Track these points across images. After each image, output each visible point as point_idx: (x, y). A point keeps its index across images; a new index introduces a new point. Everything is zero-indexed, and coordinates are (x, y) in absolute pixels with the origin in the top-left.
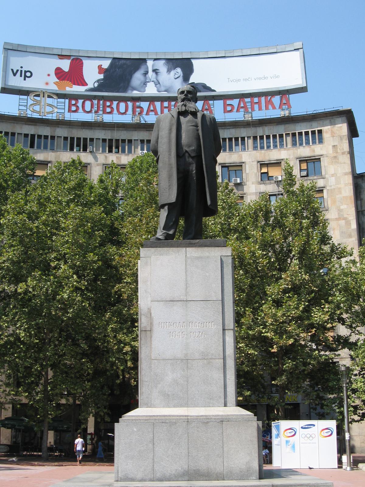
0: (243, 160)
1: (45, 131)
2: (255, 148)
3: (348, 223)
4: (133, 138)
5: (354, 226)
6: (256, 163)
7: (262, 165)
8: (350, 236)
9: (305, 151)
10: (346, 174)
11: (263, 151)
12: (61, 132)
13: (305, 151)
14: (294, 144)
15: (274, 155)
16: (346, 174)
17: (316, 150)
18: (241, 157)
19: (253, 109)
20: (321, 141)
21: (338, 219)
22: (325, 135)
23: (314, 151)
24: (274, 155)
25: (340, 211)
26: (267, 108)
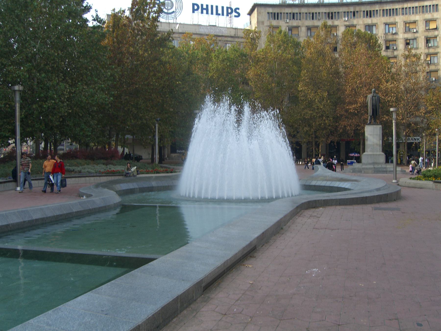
0: (397, 21)
1: (296, 10)
2: (403, 14)
4: (340, 11)
6: (403, 22)
7: (406, 23)
9: (428, 16)
11: (407, 16)
13: (428, 16)
14: (423, 12)
15: (413, 18)
20: (437, 10)
23: (433, 16)
24: (413, 18)
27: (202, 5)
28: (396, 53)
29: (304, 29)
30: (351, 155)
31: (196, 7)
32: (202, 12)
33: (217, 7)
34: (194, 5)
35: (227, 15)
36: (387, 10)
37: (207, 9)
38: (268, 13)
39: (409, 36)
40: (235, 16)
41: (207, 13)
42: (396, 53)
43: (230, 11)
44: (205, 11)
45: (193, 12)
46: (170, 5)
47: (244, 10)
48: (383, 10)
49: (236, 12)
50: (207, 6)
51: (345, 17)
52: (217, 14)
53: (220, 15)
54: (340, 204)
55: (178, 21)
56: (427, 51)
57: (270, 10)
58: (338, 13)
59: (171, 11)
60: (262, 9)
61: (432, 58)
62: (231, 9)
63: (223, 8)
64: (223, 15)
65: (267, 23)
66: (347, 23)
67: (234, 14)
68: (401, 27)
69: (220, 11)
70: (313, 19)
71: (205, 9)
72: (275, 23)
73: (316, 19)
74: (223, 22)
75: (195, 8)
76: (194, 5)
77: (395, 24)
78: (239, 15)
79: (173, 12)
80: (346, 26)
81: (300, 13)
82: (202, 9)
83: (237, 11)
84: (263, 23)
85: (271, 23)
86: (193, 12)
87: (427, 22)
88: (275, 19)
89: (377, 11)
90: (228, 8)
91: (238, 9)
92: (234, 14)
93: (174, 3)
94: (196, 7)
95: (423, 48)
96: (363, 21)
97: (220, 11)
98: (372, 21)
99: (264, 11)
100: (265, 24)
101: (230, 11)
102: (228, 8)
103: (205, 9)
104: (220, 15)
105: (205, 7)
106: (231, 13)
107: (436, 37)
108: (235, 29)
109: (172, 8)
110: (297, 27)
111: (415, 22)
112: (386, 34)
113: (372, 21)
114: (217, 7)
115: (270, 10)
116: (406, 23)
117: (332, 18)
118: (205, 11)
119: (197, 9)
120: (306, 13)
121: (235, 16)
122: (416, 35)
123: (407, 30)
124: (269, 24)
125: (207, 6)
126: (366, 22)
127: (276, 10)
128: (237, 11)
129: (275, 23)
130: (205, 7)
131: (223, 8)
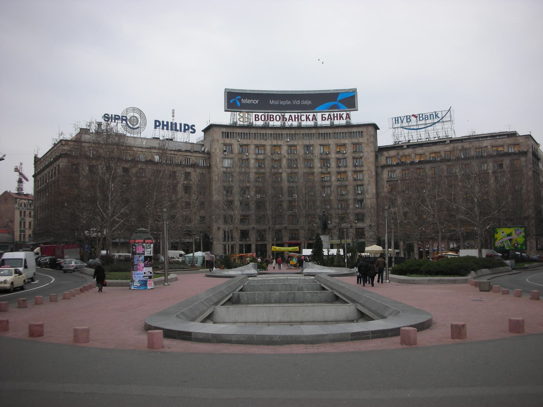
3: (371, 172)
5: (374, 174)
7: (337, 145)
8: (372, 178)
10: (372, 151)
12: (253, 131)
13: (355, 141)
16: (372, 151)
17: (361, 140)
19: (334, 119)
20: (362, 136)
21: (367, 170)
22: (364, 134)
24: (343, 141)
25: (368, 167)
26: (340, 119)
27: (163, 122)
28: (329, 170)
29: (252, 147)
31: (158, 124)
32: (163, 129)
34: (156, 121)
35: (185, 131)
37: (167, 125)
38: (223, 132)
39: (340, 156)
40: (191, 132)
42: (329, 170)
43: (187, 127)
44: (165, 127)
45: (155, 128)
47: (200, 127)
48: (319, 134)
53: (178, 131)
54: (373, 338)
55: (143, 136)
56: (354, 169)
57: (224, 130)
58: (282, 134)
59: (136, 127)
61: (358, 175)
63: (181, 124)
64: (181, 131)
66: (289, 143)
69: (178, 128)
72: (228, 141)
73: (263, 139)
74: (180, 137)
75: (157, 124)
76: (156, 121)
78: (194, 131)
79: (138, 127)
81: (250, 133)
82: (163, 125)
85: (225, 141)
86: (155, 128)
87: (355, 144)
88: (228, 137)
91: (194, 126)
92: (190, 130)
93: (139, 120)
94: (158, 124)
95: (351, 166)
97: (178, 128)
100: (220, 142)
101: (187, 127)
102: (185, 125)
104: (178, 131)
106: (188, 129)
107: (361, 158)
108: (192, 143)
109: (137, 124)
110: (247, 145)
116: (337, 145)
117: (276, 139)
118: (165, 127)
120: (255, 134)
121: (191, 132)
122: (345, 156)
125: (167, 122)
126: (304, 143)
127: (229, 130)
129: (228, 141)
131: (181, 124)
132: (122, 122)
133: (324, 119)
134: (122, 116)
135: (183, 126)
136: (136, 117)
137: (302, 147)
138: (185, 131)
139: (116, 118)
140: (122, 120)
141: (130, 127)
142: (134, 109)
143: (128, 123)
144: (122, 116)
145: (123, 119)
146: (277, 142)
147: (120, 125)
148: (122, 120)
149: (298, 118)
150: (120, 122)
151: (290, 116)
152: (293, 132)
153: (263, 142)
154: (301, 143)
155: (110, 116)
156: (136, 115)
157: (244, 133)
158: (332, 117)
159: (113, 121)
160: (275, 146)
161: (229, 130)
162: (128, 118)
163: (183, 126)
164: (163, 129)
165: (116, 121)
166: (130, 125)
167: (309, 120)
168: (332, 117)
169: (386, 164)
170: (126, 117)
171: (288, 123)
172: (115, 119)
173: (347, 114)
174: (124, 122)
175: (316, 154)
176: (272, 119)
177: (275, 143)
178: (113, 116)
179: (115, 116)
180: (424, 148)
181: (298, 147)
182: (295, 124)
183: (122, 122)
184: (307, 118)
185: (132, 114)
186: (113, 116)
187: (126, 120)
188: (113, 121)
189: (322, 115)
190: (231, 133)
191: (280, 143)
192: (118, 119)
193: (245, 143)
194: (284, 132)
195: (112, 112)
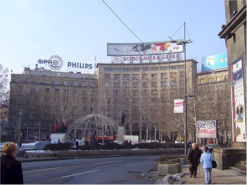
7: (171, 73)
18: (166, 71)
27: (73, 63)
29: (122, 76)
30: (99, 143)
31: (70, 64)
32: (73, 67)
33: (80, 64)
34: (69, 63)
35: (86, 68)
36: (162, 67)
37: (75, 65)
40: (90, 68)
41: (75, 67)
43: (87, 66)
44: (74, 66)
45: (68, 66)
46: (57, 63)
49: (90, 66)
50: (75, 63)
51: (142, 70)
52: (81, 67)
53: (82, 67)
55: (60, 71)
57: (106, 66)
60: (101, 66)
62: (88, 65)
64: (83, 68)
65: (104, 73)
67: (89, 67)
68: (168, 76)
69: (82, 66)
70: (126, 71)
71: (74, 65)
74: (84, 71)
75: (69, 64)
76: (69, 63)
77: (166, 74)
79: (58, 66)
80: (142, 74)
82: (73, 65)
83: (91, 65)
84: (102, 72)
85: (105, 73)
87: (181, 72)
88: (108, 71)
89: (157, 67)
90: (86, 64)
91: (91, 65)
92: (89, 67)
93: (59, 62)
94: (70, 64)
96: (151, 72)
97: (82, 66)
98: (155, 72)
99: (103, 67)
100: (103, 73)
101: (87, 66)
102: (86, 64)
103: (74, 65)
104: (82, 67)
105: (74, 64)
106: (88, 67)
108: (89, 74)
110: (119, 75)
111: (175, 73)
112: (161, 78)
113: (155, 72)
114: (80, 64)
115: (106, 66)
116: (171, 73)
117: (136, 71)
118: (74, 66)
119: (70, 65)
121: (90, 68)
123: (172, 77)
124: (104, 73)
125: (75, 63)
127: (109, 67)
128: (91, 65)
129: (107, 73)
130: (74, 64)
131: (83, 64)
132: (49, 64)
133: (164, 58)
134: (49, 61)
135: (85, 65)
136: (57, 61)
137: (151, 75)
138: (86, 68)
139: (46, 61)
140: (49, 62)
141: (53, 66)
142: (56, 56)
143: (52, 64)
144: (49, 61)
145: (50, 62)
146: (136, 73)
147: (48, 65)
148: (49, 62)
149: (149, 58)
150: (48, 63)
151: (144, 57)
152: (145, 66)
153: (128, 73)
154: (150, 73)
155: (42, 60)
156: (57, 59)
157: (117, 68)
158: (169, 57)
159: (44, 63)
160: (135, 75)
161: (109, 67)
162: (52, 61)
163: (85, 65)
164: (73, 67)
165: (45, 63)
166: (53, 65)
167: (155, 59)
168: (169, 57)
169: (200, 83)
170: (51, 61)
171: (144, 62)
172: (45, 62)
173: (177, 54)
174: (50, 63)
175: (158, 79)
176: (134, 59)
177: (135, 73)
178: (44, 61)
179: (45, 60)
180: (222, 73)
181: (148, 75)
182: (148, 61)
183: (49, 64)
184: (154, 58)
185: (55, 59)
186: (44, 61)
187: (51, 63)
188: (44, 63)
189: (163, 56)
190: (109, 68)
191: (138, 73)
192: (46, 62)
193: (117, 74)
194: (140, 66)
195: (43, 58)
